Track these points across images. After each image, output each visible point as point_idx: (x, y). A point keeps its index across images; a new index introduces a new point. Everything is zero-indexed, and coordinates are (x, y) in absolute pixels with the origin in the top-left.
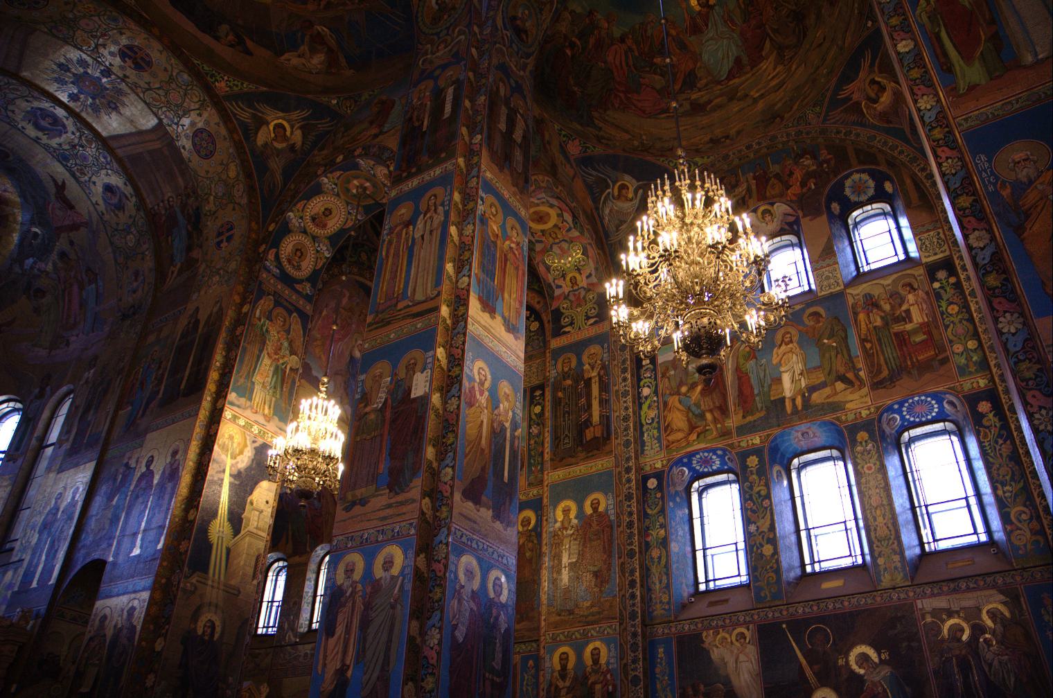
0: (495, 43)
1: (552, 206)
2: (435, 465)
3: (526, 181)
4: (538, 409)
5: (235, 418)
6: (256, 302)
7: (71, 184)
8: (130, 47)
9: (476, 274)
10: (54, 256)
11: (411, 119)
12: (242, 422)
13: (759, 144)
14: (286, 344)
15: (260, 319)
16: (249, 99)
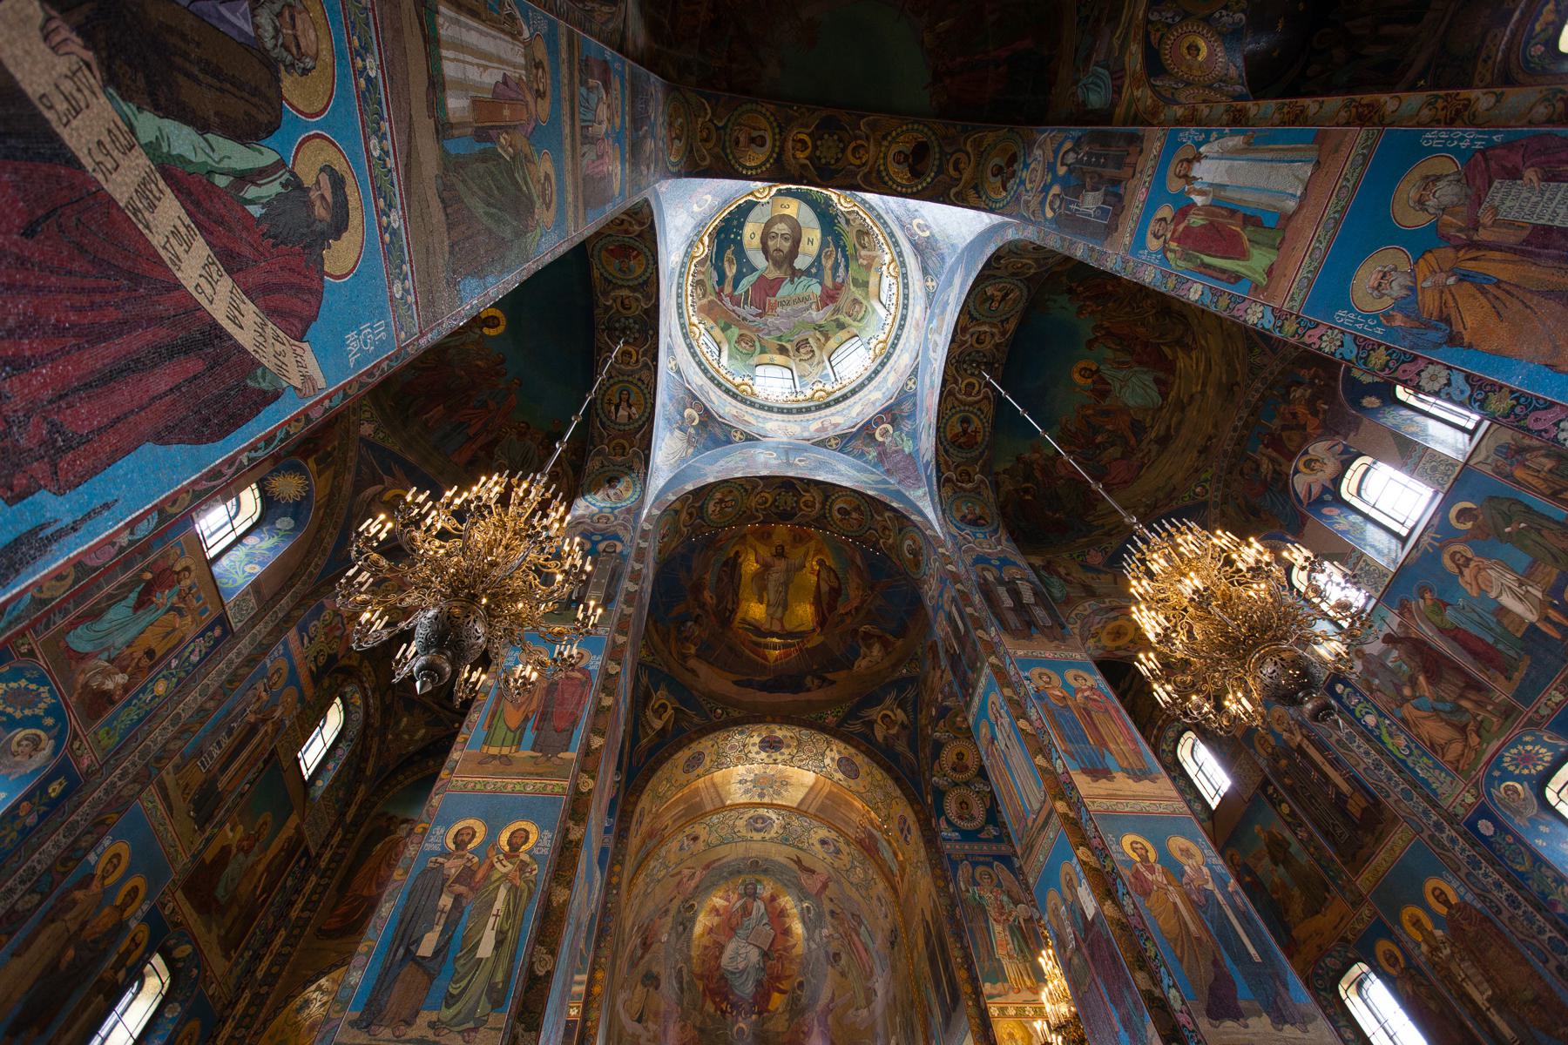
0: (960, 549)
1: (1115, 619)
2: (1157, 992)
3: (1063, 627)
4: (1285, 809)
5: (1002, 1010)
6: (955, 876)
7: (802, 855)
8: (761, 742)
9: (1065, 751)
10: (828, 918)
11: (947, 651)
12: (1012, 1012)
13: (1240, 418)
14: (1005, 898)
15: (968, 891)
16: (852, 714)
